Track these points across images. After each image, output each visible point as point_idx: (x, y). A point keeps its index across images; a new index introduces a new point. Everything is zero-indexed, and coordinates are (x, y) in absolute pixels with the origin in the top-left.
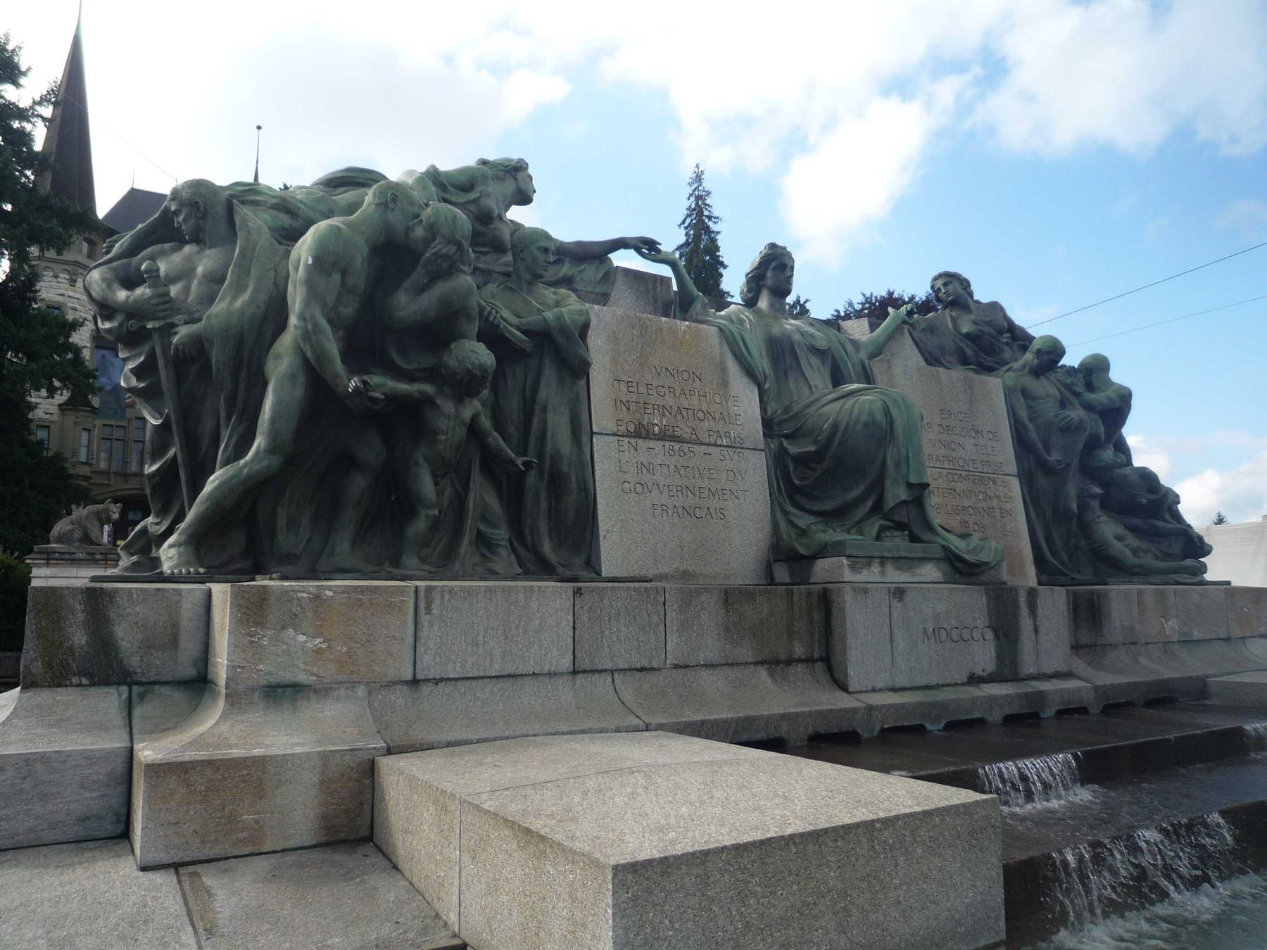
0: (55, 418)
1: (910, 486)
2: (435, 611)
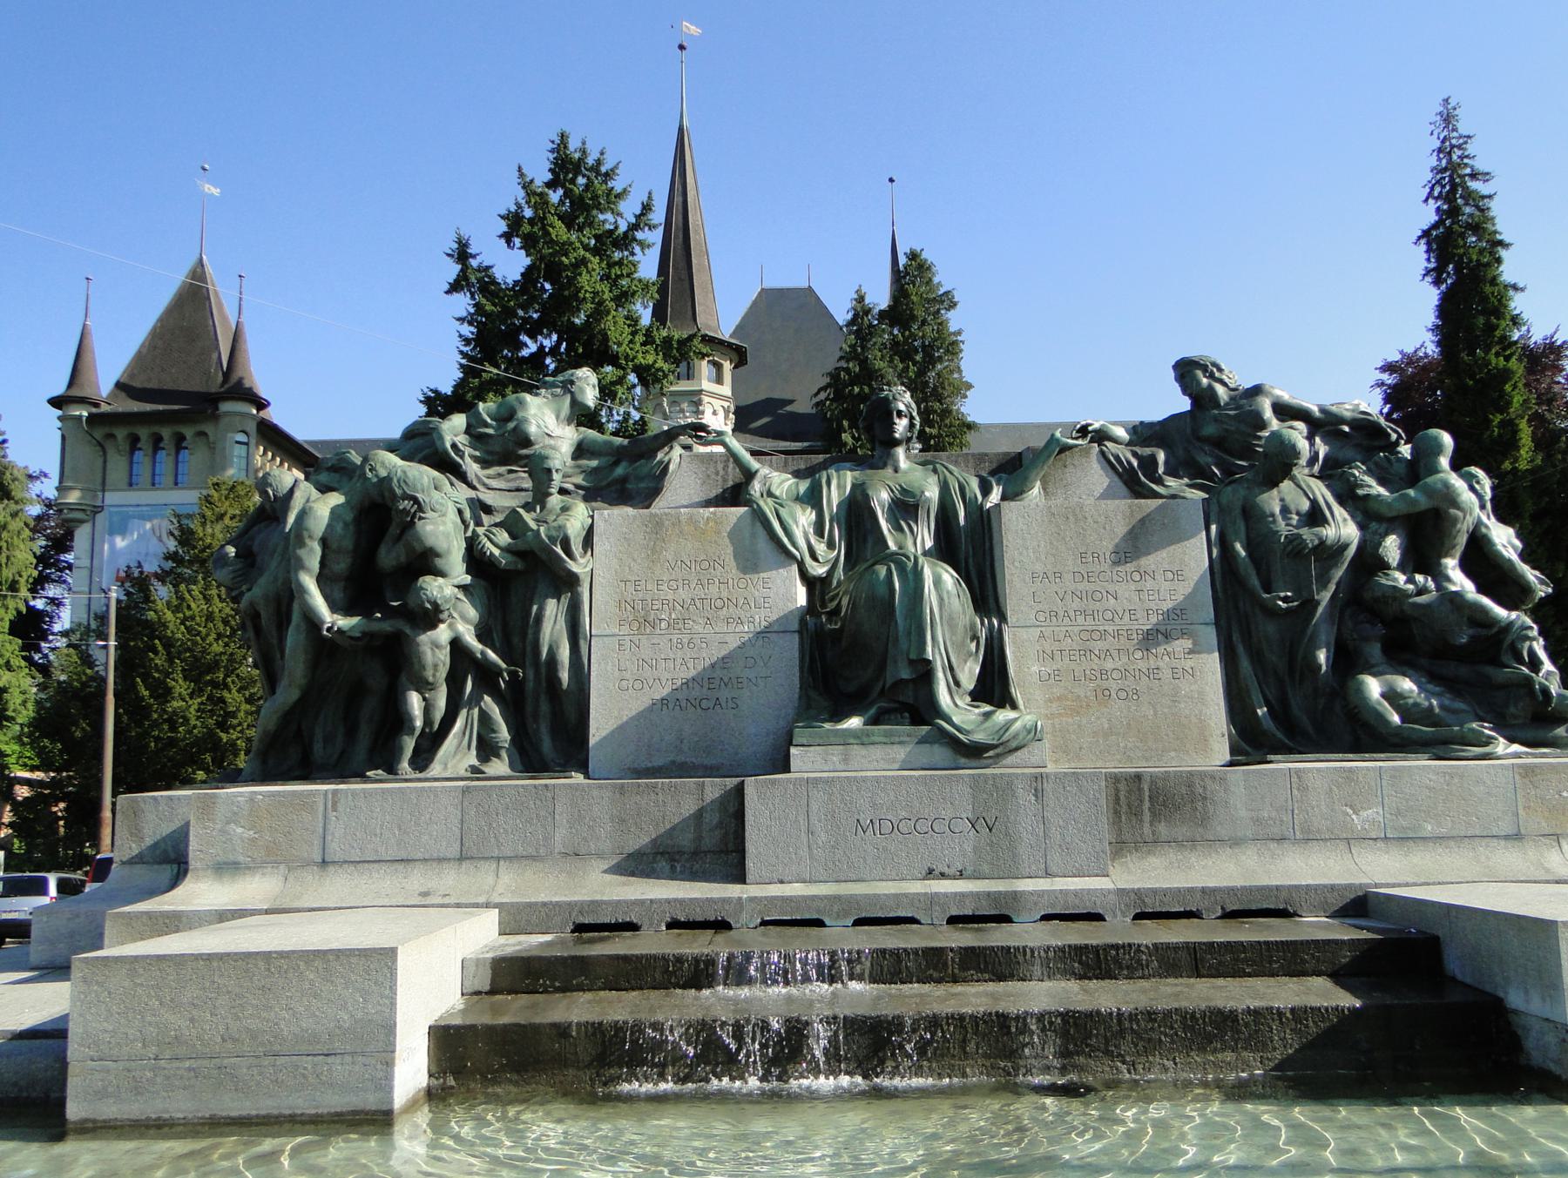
1: (911, 662)
2: (340, 809)
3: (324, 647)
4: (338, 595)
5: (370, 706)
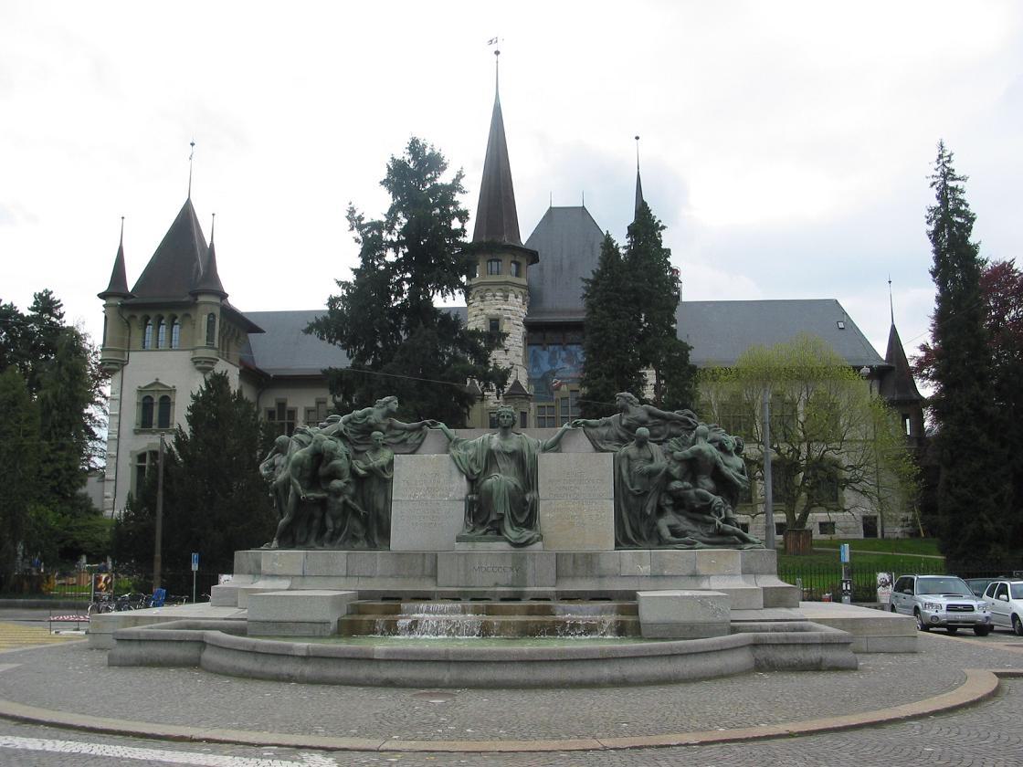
3: (300, 503)
5: (316, 522)
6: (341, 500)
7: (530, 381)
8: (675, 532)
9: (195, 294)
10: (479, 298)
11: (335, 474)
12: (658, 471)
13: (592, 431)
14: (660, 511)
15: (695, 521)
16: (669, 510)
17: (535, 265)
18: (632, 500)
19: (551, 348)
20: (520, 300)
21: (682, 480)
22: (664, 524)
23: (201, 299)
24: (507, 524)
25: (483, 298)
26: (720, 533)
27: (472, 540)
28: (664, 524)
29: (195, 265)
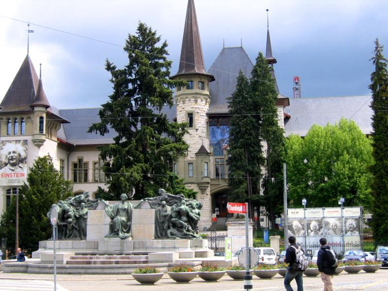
0: (194, 159)
4: (60, 220)
5: (64, 232)
6: (71, 225)
7: (211, 145)
8: (172, 234)
9: (33, 107)
10: (181, 102)
11: (69, 217)
12: (168, 215)
13: (150, 201)
14: (169, 228)
15: (179, 231)
16: (171, 227)
17: (213, 82)
18: (160, 224)
19: (222, 127)
20: (204, 102)
21: (175, 218)
22: (169, 232)
23: (36, 109)
24: (120, 231)
25: (184, 102)
26: (186, 235)
27: (109, 237)
28: (169, 232)
29: (32, 90)
